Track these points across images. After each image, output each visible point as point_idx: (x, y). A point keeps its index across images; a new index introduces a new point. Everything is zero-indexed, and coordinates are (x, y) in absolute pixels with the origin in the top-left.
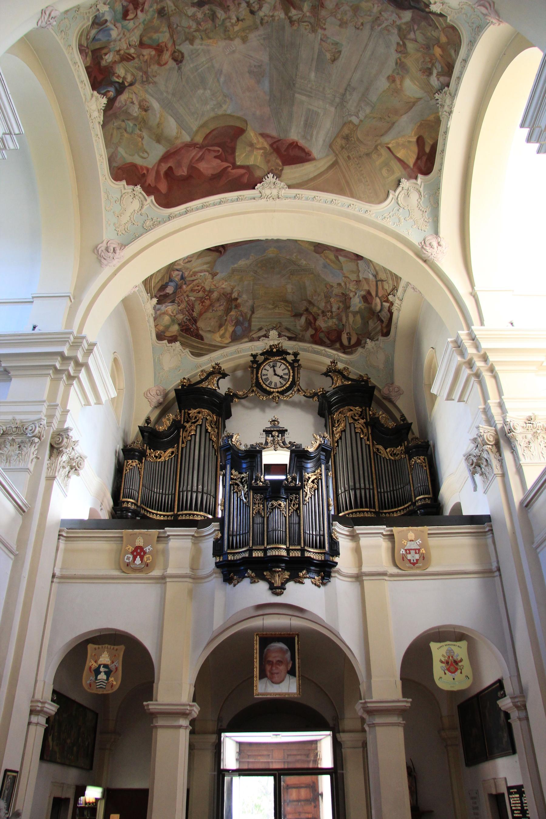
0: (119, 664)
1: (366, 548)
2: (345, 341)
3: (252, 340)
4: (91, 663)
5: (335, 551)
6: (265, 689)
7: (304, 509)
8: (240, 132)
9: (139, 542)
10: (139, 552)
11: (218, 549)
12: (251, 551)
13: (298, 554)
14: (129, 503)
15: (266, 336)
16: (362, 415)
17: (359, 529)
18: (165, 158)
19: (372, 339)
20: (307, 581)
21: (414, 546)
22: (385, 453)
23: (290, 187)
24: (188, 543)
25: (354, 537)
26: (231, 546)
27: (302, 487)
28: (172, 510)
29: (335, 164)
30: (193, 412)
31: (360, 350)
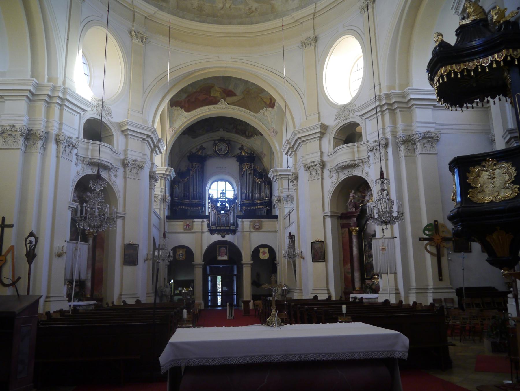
0: (184, 253)
1: (246, 224)
2: (247, 134)
3: (213, 132)
4: (178, 253)
5: (237, 225)
6: (220, 258)
7: (230, 216)
8: (213, 87)
9: (188, 223)
10: (188, 225)
11: (208, 224)
12: (217, 227)
13: (228, 228)
14: (176, 200)
15: (219, 130)
16: (251, 167)
17: (244, 220)
18: (188, 97)
19: (257, 135)
20: (230, 234)
21: (257, 224)
22: (257, 180)
23: (228, 104)
24: (200, 223)
25: (242, 222)
26: (212, 225)
27: (230, 209)
28: (189, 199)
29: (243, 98)
30: (194, 164)
31: (252, 138)
